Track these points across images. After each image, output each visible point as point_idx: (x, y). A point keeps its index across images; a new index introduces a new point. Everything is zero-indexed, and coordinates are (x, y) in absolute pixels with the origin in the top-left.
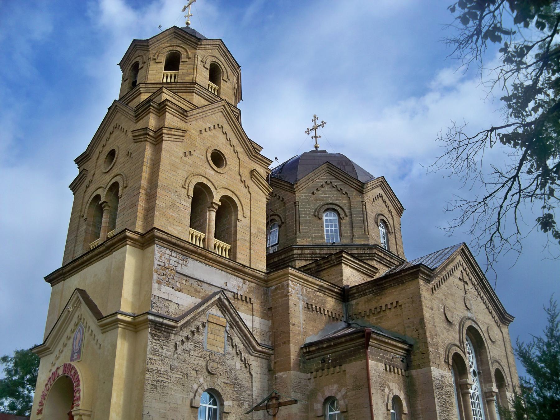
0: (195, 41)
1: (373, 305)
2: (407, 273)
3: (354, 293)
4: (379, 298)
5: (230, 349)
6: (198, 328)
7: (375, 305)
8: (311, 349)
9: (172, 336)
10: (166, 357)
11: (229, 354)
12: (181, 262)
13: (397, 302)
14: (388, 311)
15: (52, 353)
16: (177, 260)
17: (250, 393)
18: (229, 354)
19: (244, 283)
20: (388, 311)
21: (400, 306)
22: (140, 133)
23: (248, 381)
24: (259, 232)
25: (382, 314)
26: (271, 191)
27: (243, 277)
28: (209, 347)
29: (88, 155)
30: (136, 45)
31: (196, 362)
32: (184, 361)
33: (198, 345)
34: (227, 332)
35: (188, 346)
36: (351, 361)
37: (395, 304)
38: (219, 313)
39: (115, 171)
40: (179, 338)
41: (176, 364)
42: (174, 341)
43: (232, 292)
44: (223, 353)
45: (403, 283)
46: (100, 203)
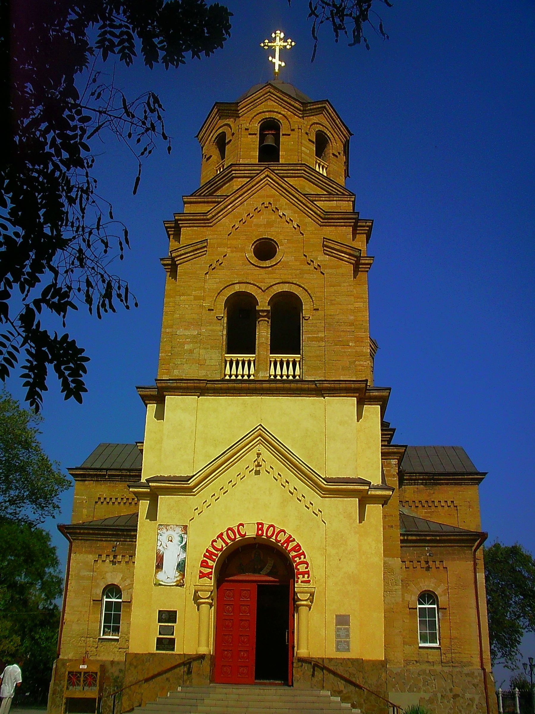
0: (345, 133)
1: (423, 497)
2: (471, 477)
3: (406, 480)
4: (432, 492)
7: (428, 499)
8: (410, 538)
13: (452, 502)
14: (439, 507)
15: (195, 495)
20: (439, 507)
21: (457, 506)
22: (345, 250)
25: (433, 509)
29: (208, 220)
30: (269, 92)
36: (454, 560)
37: (449, 503)
39: (280, 274)
45: (461, 484)
46: (257, 308)
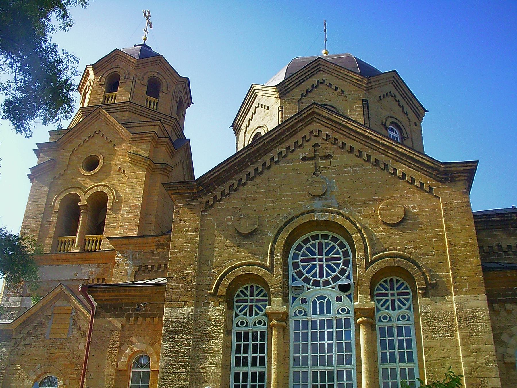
5: (75, 332)
11: (73, 337)
19: (98, 266)
24: (132, 209)
26: (148, 162)
27: (96, 262)
38: (65, 303)
44: (66, 337)
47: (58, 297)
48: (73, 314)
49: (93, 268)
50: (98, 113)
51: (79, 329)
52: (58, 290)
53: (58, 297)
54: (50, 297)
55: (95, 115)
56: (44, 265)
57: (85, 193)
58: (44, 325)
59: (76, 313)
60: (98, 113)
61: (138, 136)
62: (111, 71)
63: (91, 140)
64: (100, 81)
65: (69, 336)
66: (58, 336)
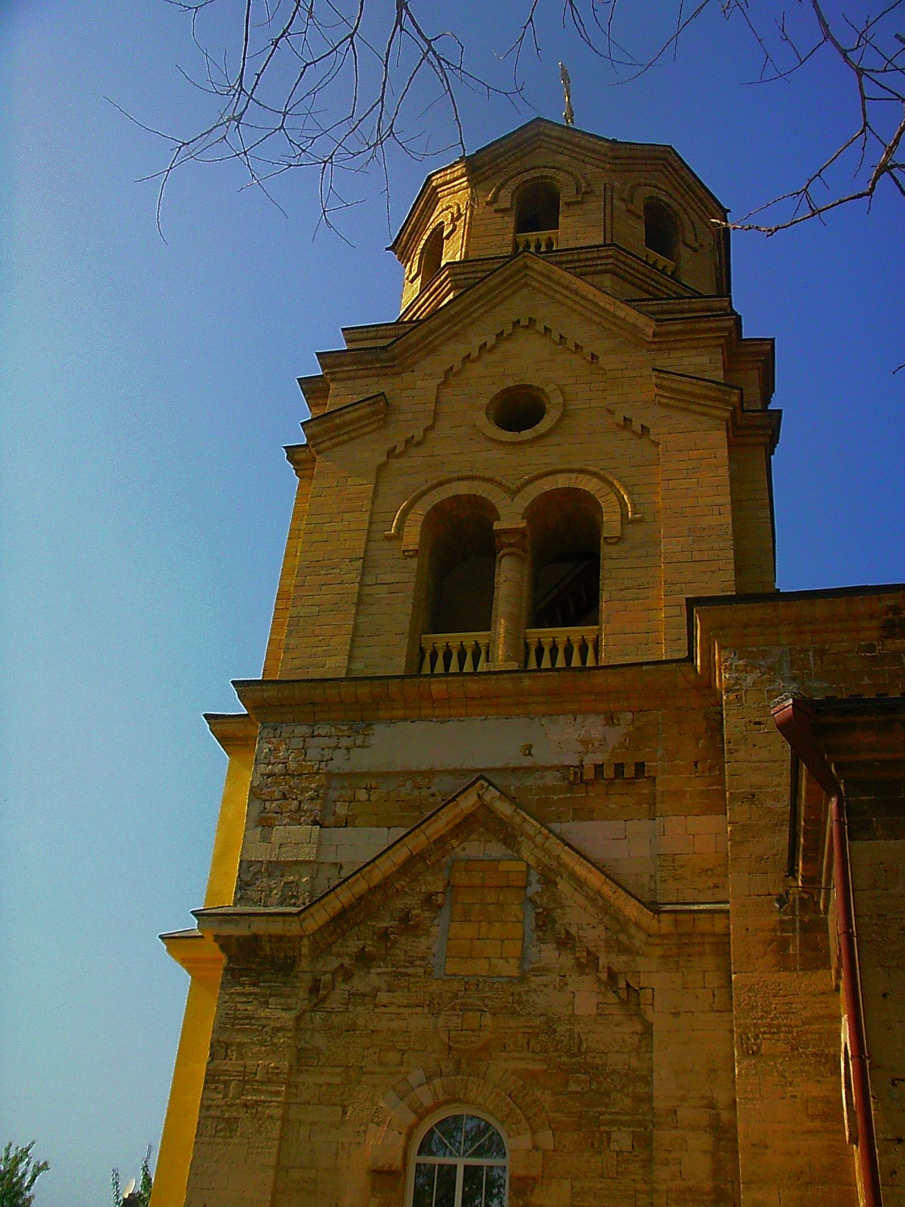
5: (549, 954)
6: (405, 918)
9: (304, 964)
10: (279, 1029)
11: (541, 971)
12: (345, 742)
16: (333, 742)
17: (641, 1089)
18: (541, 971)
23: (637, 1050)
28: (453, 967)
31: (395, 1025)
32: (352, 1028)
33: (410, 971)
34: (530, 899)
35: (372, 979)
38: (496, 850)
40: (333, 963)
41: (320, 1041)
42: (308, 976)
43: (552, 767)
44: (515, 972)
47: (464, 827)
48: (535, 888)
49: (594, 727)
50: (519, 271)
51: (565, 942)
52: (468, 802)
53: (464, 827)
54: (441, 824)
55: (511, 276)
56: (392, 720)
57: (514, 493)
58: (416, 927)
59: (548, 881)
60: (519, 271)
61: (680, 327)
62: (527, 176)
63: (506, 347)
64: (495, 199)
65: (527, 967)
66: (482, 967)
